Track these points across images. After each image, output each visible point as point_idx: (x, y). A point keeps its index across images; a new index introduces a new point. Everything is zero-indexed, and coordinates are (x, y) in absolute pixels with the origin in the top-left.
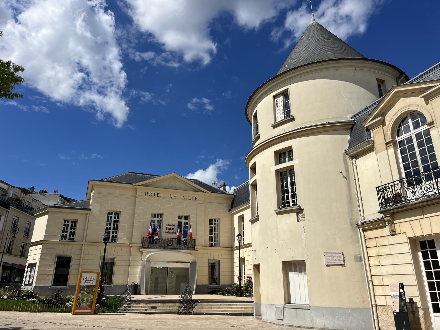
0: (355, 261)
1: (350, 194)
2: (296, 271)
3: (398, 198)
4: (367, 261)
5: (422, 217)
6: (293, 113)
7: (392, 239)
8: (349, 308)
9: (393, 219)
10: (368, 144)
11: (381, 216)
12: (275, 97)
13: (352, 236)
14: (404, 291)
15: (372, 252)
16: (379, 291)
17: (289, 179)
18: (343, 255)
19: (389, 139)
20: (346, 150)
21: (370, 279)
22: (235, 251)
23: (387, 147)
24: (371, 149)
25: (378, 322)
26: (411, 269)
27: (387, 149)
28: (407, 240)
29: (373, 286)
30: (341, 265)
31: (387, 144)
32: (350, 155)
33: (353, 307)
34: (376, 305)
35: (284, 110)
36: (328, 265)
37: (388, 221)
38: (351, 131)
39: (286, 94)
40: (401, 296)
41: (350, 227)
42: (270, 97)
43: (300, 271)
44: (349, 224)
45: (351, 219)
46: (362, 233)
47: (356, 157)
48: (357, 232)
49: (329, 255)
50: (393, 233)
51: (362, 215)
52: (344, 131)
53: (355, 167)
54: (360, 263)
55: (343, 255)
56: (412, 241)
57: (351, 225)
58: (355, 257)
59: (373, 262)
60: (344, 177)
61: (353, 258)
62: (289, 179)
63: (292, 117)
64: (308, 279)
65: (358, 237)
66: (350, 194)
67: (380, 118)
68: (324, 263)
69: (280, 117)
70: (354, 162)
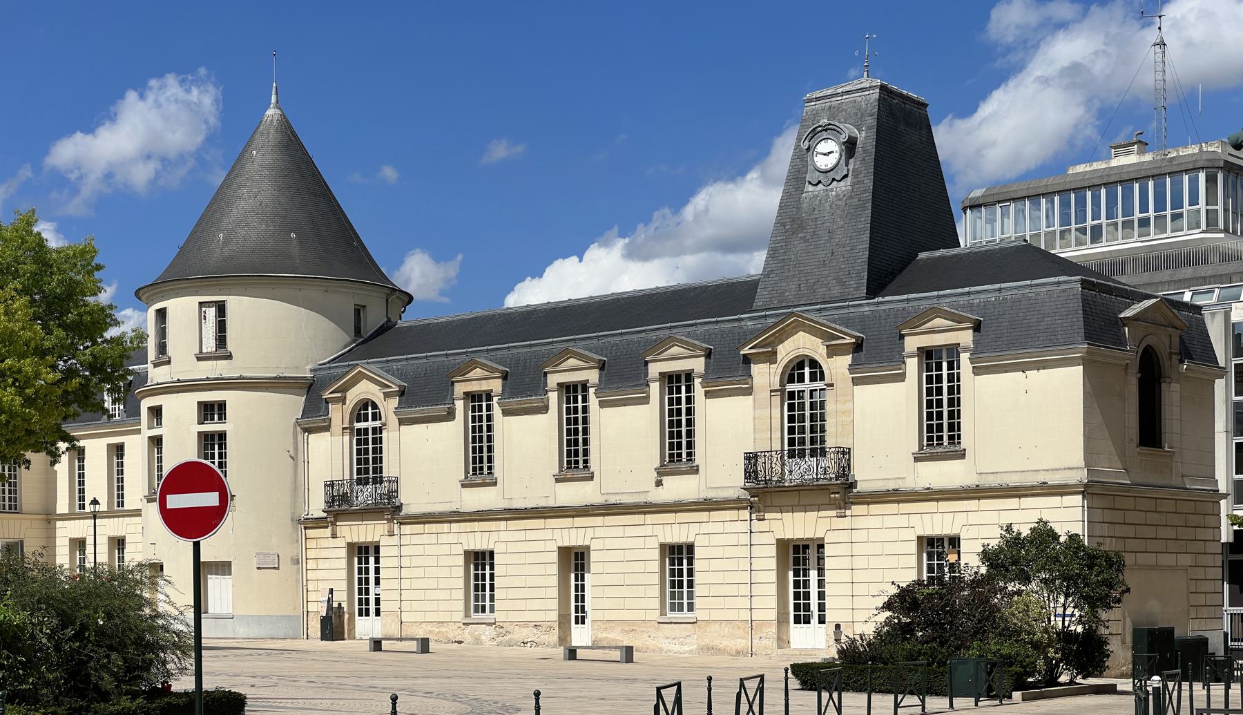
0: (292, 564)
1: (295, 481)
2: (217, 574)
3: (345, 498)
4: (304, 564)
5: (360, 523)
6: (231, 346)
7: (332, 542)
8: (278, 616)
9: (336, 520)
10: (323, 423)
11: (325, 515)
12: (201, 303)
13: (291, 534)
14: (332, 596)
15: (311, 554)
16: (312, 597)
17: (216, 447)
18: (278, 556)
19: (346, 425)
20: (298, 419)
21: (305, 584)
22: (57, 522)
23: (343, 433)
24: (327, 428)
25: (308, 629)
26: (344, 574)
27: (343, 435)
28: (345, 545)
29: (307, 591)
30: (274, 568)
31: (343, 429)
32: (302, 426)
33: (282, 614)
34: (308, 612)
35: (216, 332)
36: (258, 568)
37: (331, 522)
38: (308, 391)
39: (221, 308)
40: (330, 601)
41: (290, 522)
42: (194, 301)
43: (223, 574)
44: (290, 518)
45: (293, 513)
46: (303, 530)
47: (309, 431)
48: (298, 529)
49: (261, 556)
50: (334, 536)
51: (306, 509)
52: (298, 391)
53: (306, 444)
54: (296, 566)
55: (278, 556)
56: (350, 546)
57: (292, 520)
58: (292, 559)
59: (311, 565)
60: (291, 457)
61: (289, 560)
62: (216, 447)
63: (229, 354)
64: (234, 583)
65: (298, 536)
66: (295, 481)
67: (340, 395)
68: (256, 566)
69: (210, 345)
70: (305, 437)
